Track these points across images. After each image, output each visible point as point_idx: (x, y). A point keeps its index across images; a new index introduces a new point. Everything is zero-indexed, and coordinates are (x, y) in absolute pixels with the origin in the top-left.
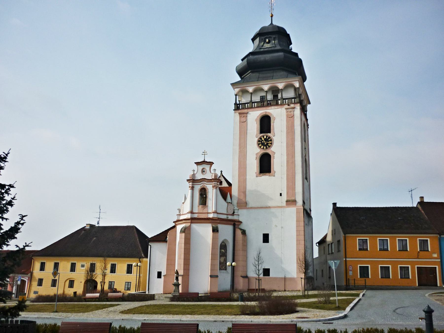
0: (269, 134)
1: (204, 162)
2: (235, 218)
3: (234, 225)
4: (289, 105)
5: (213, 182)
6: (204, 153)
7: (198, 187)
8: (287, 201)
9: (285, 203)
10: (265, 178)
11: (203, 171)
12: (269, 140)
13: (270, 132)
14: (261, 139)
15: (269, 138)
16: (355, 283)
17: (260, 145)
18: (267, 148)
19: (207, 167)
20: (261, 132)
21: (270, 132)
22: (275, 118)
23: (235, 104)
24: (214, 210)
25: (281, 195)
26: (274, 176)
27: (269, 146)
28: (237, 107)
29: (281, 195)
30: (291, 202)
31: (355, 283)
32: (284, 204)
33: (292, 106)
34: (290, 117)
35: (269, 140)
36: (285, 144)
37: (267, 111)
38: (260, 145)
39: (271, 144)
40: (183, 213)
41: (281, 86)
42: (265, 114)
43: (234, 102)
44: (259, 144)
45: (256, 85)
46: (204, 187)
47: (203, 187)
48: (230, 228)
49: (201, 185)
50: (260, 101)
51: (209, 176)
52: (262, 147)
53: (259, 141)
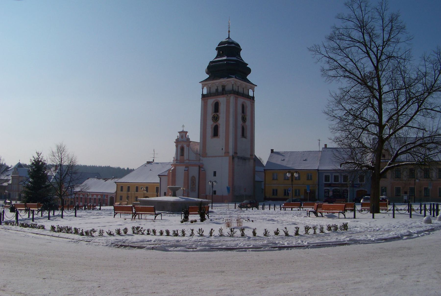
0: (218, 113)
1: (183, 132)
2: (201, 162)
3: (199, 166)
4: (227, 95)
7: (179, 146)
8: (225, 153)
10: (215, 139)
11: (182, 137)
13: (218, 112)
14: (214, 116)
15: (218, 115)
17: (213, 120)
18: (216, 122)
19: (184, 134)
21: (218, 112)
23: (202, 95)
24: (187, 158)
25: (222, 149)
27: (218, 121)
28: (203, 96)
29: (222, 149)
30: (227, 153)
32: (223, 155)
33: (229, 95)
34: (228, 103)
36: (225, 119)
37: (218, 99)
38: (213, 120)
39: (218, 119)
42: (215, 102)
43: (202, 93)
44: (213, 119)
48: (197, 168)
51: (184, 139)
53: (213, 117)
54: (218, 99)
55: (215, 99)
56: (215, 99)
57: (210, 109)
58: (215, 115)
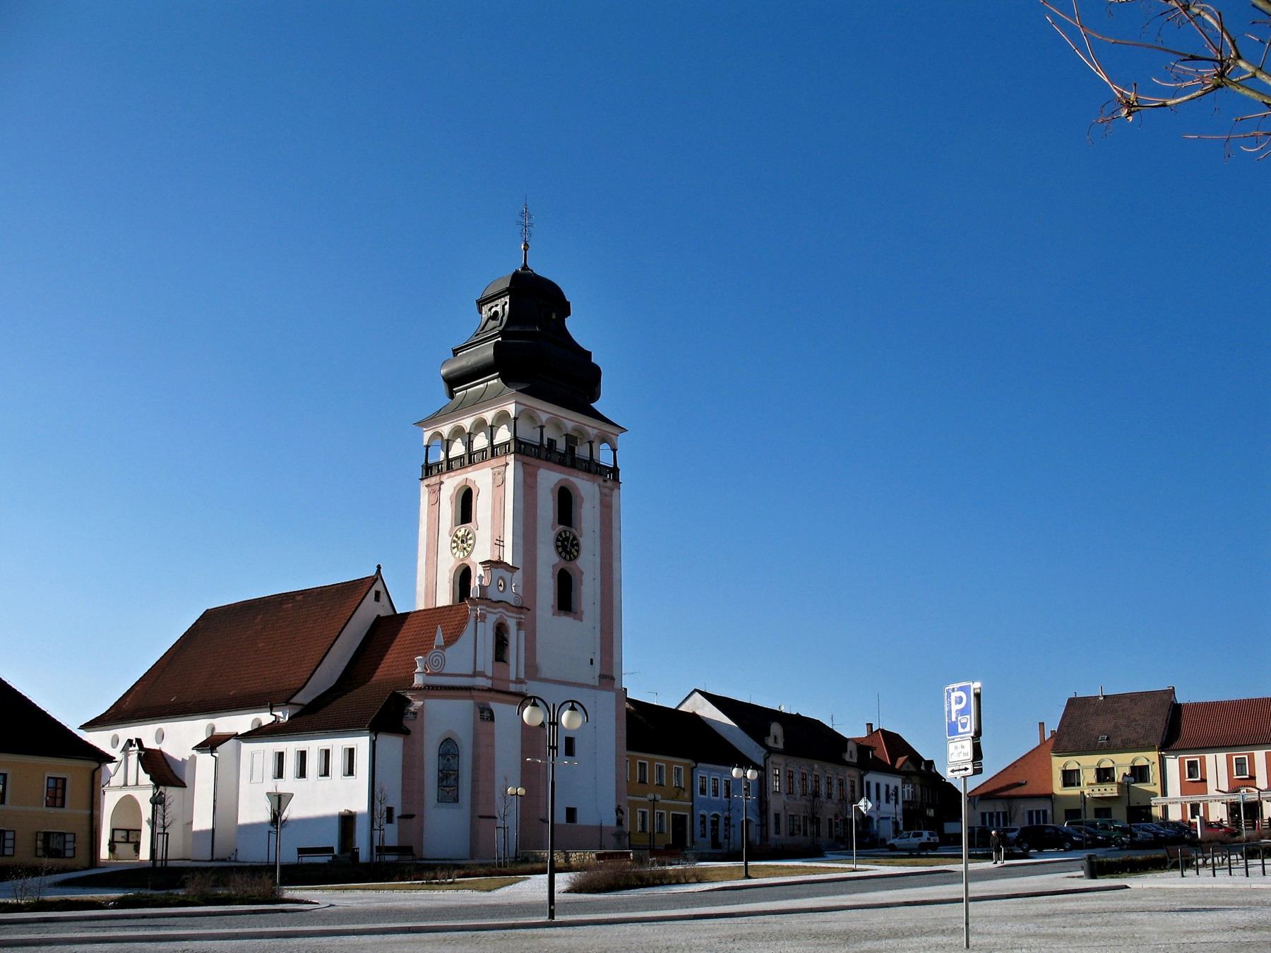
5: (521, 613)
6: (498, 542)
8: (602, 677)
9: (597, 679)
10: (566, 621)
12: (574, 543)
14: (560, 535)
15: (575, 538)
16: (1263, 865)
18: (571, 559)
20: (560, 522)
22: (583, 499)
25: (592, 660)
26: (581, 621)
29: (592, 660)
31: (1263, 865)
35: (574, 543)
36: (598, 560)
37: (573, 479)
39: (577, 551)
40: (444, 672)
41: (592, 432)
44: (558, 547)
45: (577, 422)
46: (504, 622)
47: (500, 621)
49: (498, 616)
50: (563, 452)
52: (563, 554)
53: (558, 540)
54: (573, 479)
55: (563, 476)
56: (563, 476)
57: (547, 508)
58: (565, 532)
